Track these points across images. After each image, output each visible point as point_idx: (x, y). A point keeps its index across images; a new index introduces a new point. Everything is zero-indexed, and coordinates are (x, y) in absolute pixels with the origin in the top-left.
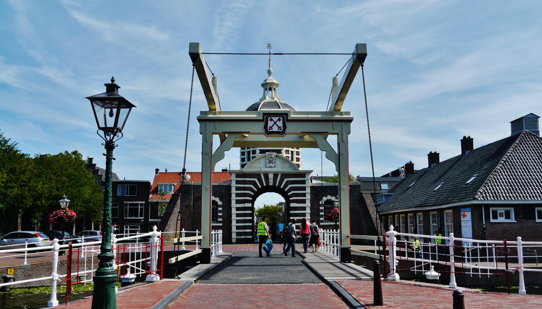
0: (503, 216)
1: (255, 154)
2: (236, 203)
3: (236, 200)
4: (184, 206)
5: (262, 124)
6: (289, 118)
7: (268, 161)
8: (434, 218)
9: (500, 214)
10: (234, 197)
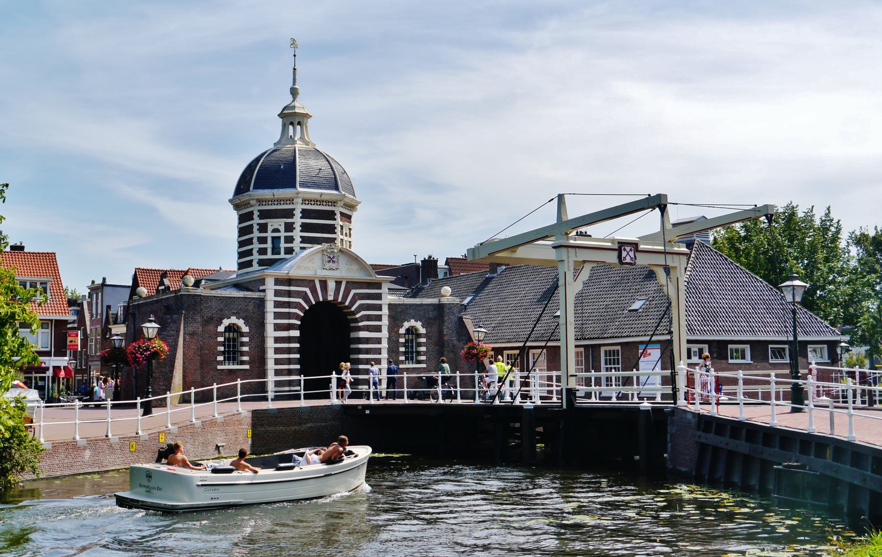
0: (696, 355)
1: (292, 243)
2: (275, 330)
4: (188, 334)
5: (616, 253)
6: (639, 249)
7: (328, 259)
8: (610, 356)
9: (695, 352)
10: (270, 320)
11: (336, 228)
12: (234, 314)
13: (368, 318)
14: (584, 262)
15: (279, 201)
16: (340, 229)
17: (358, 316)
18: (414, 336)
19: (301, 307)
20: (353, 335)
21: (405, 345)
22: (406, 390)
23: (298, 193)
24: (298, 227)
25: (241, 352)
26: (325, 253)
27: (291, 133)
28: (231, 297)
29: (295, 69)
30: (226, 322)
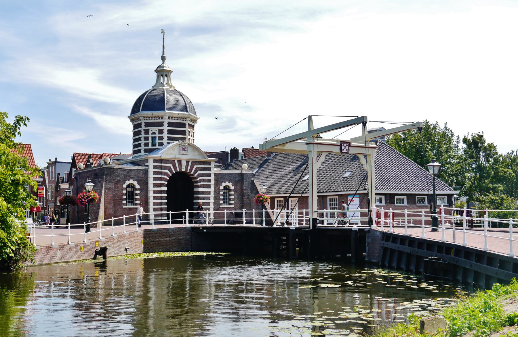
0: (378, 202)
1: (163, 140)
2: (154, 187)
3: (154, 184)
4: (107, 189)
5: (339, 147)
10: (151, 182)
11: (186, 132)
12: (132, 178)
13: (204, 181)
14: (322, 152)
15: (156, 117)
16: (188, 132)
17: (198, 179)
18: (228, 191)
19: (168, 175)
20: (195, 190)
21: (223, 195)
22: (254, 219)
23: (166, 113)
24: (166, 131)
25: (135, 198)
26: (180, 146)
27: (162, 80)
28: (130, 169)
29: (163, 46)
30: (127, 183)
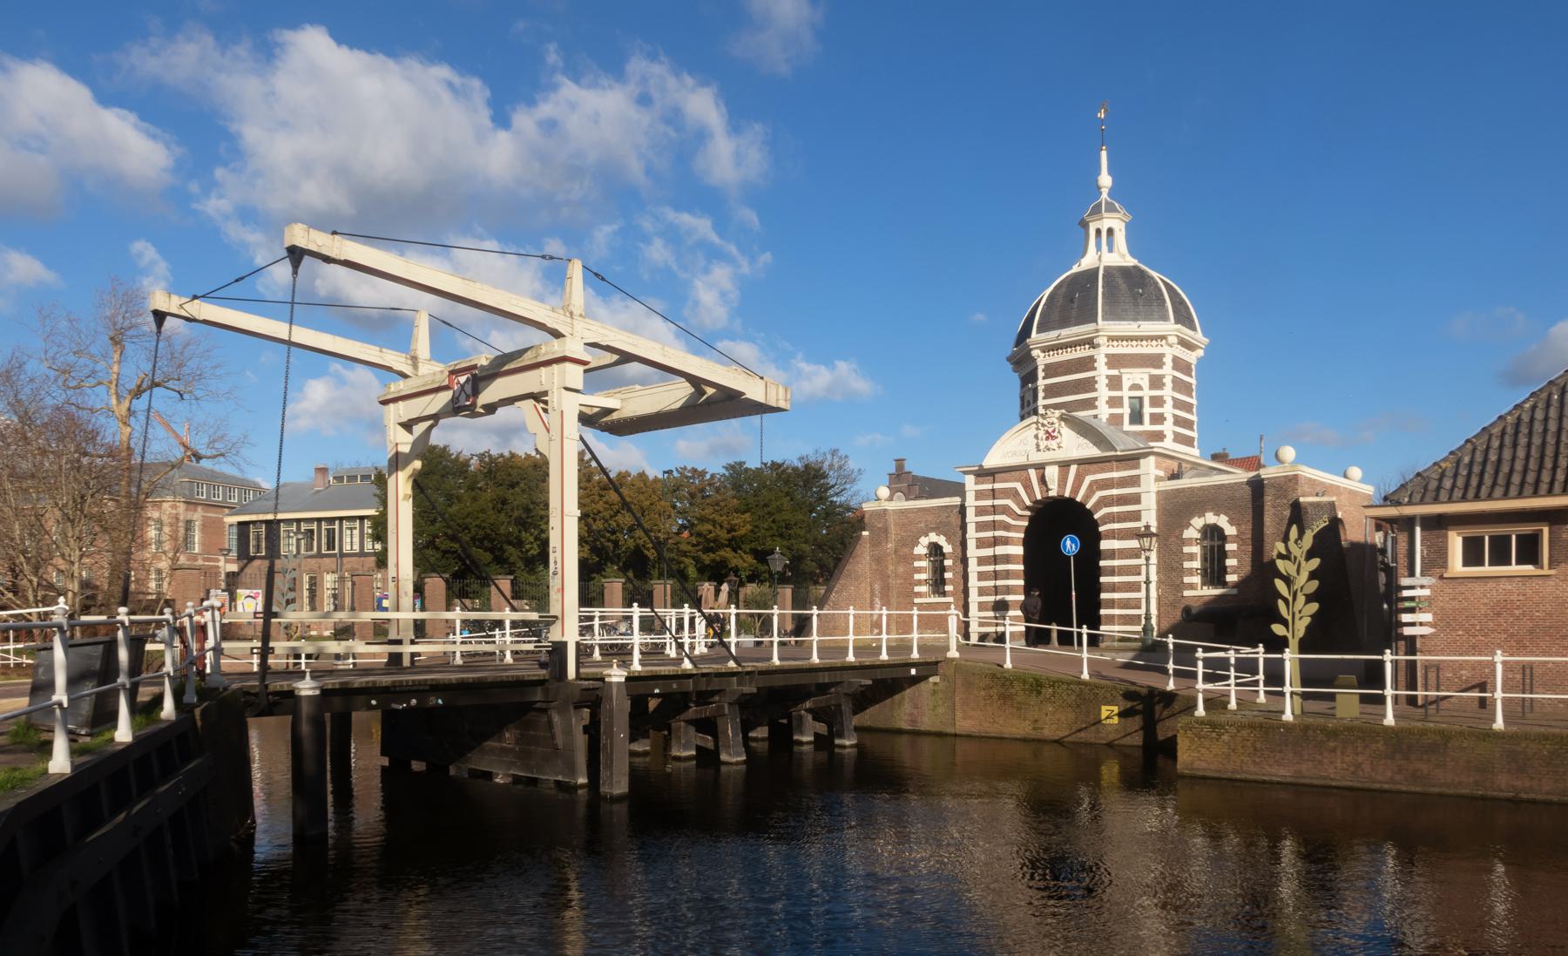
2: (978, 547)
12: (932, 530)
